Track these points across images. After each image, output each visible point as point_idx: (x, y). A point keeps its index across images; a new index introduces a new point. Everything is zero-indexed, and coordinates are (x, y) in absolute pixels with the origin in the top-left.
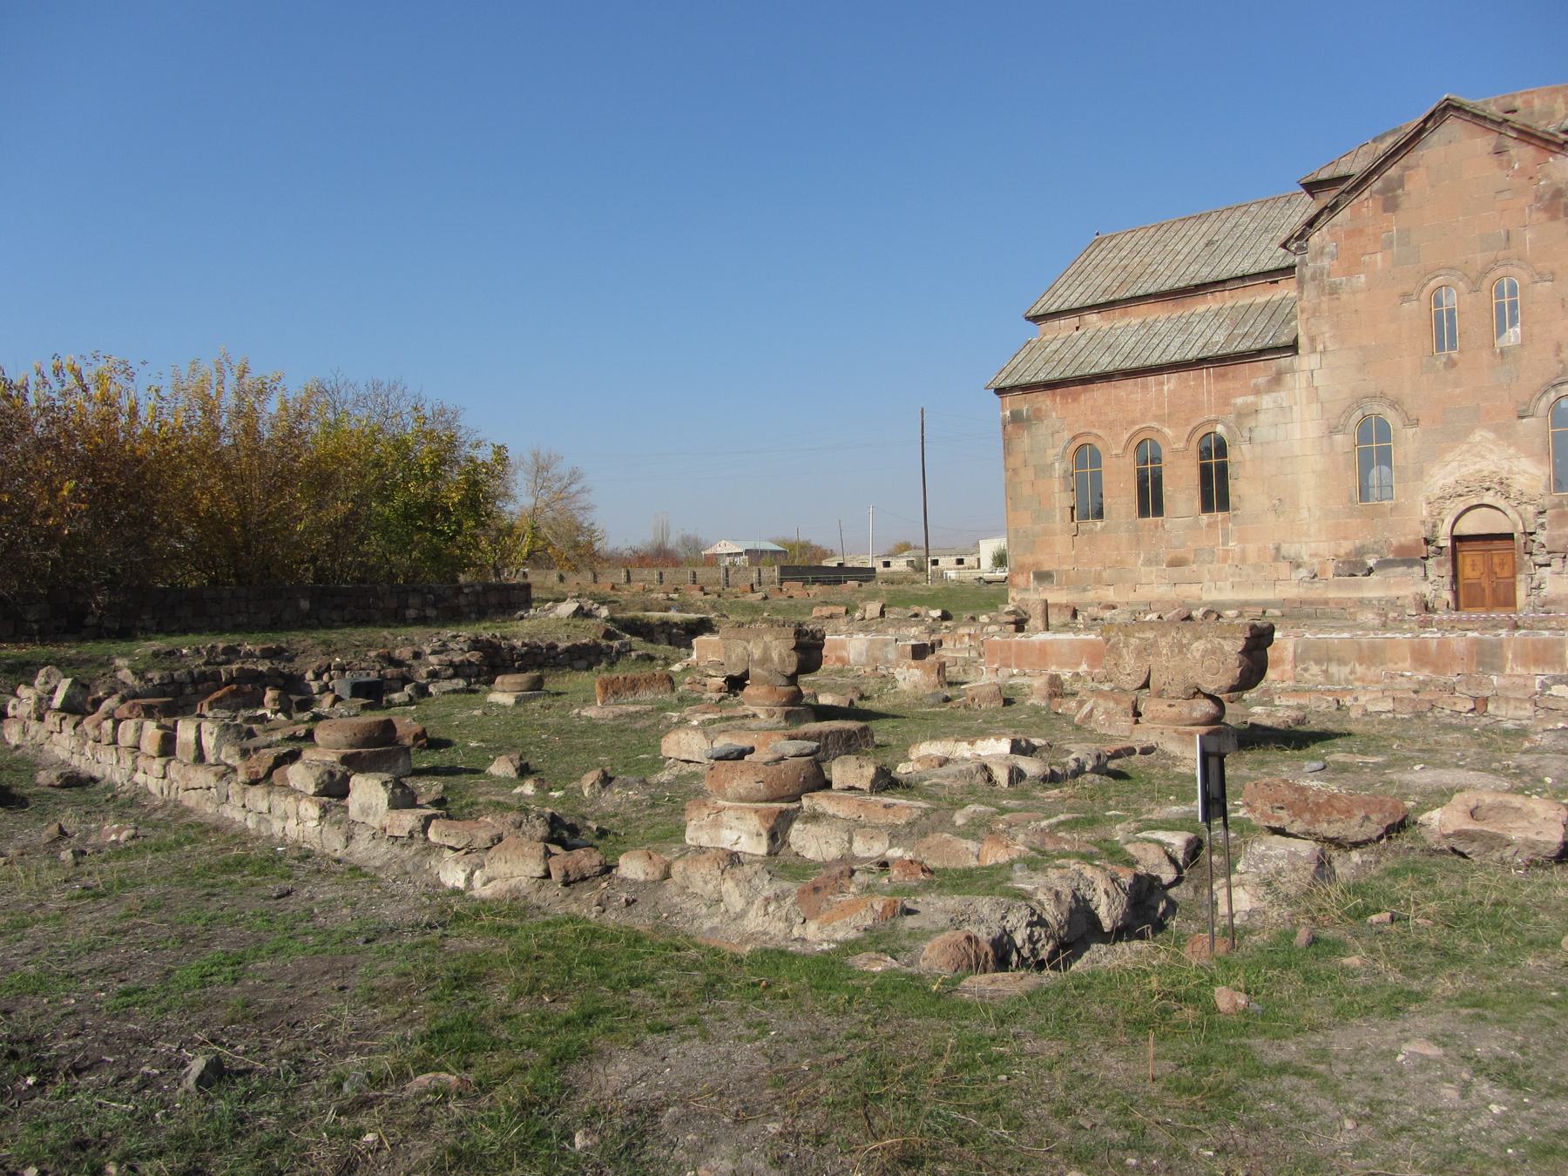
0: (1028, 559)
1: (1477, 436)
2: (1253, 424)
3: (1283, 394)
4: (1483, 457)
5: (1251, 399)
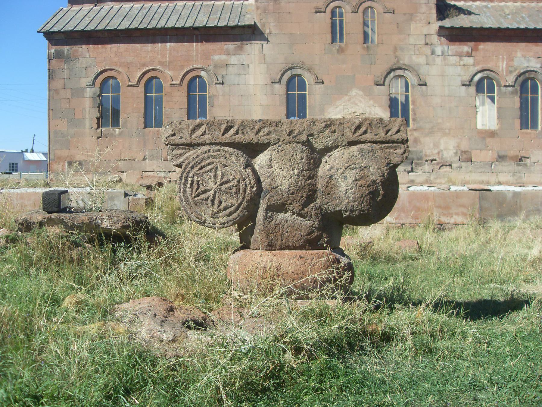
0: (64, 153)
1: (354, 92)
2: (224, 73)
3: (243, 56)
4: (356, 104)
5: (224, 57)
